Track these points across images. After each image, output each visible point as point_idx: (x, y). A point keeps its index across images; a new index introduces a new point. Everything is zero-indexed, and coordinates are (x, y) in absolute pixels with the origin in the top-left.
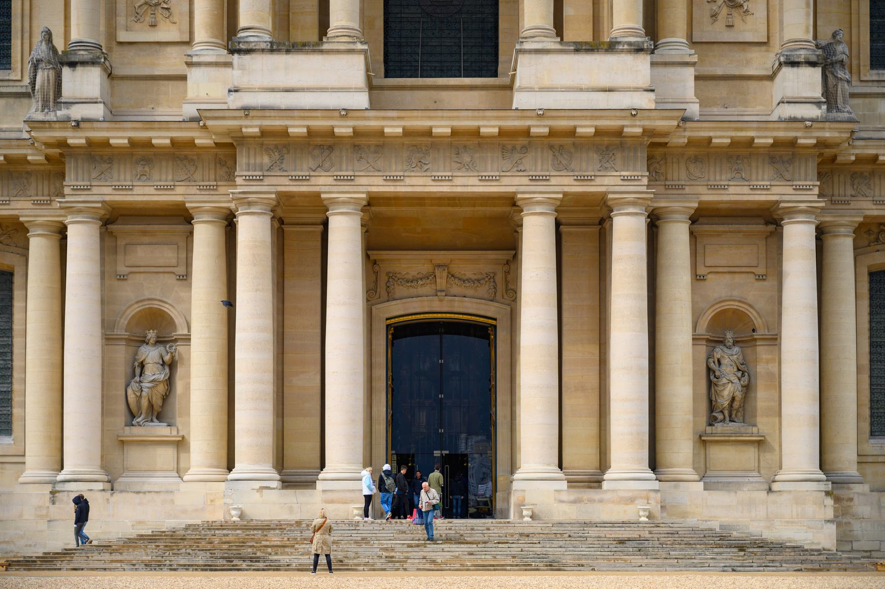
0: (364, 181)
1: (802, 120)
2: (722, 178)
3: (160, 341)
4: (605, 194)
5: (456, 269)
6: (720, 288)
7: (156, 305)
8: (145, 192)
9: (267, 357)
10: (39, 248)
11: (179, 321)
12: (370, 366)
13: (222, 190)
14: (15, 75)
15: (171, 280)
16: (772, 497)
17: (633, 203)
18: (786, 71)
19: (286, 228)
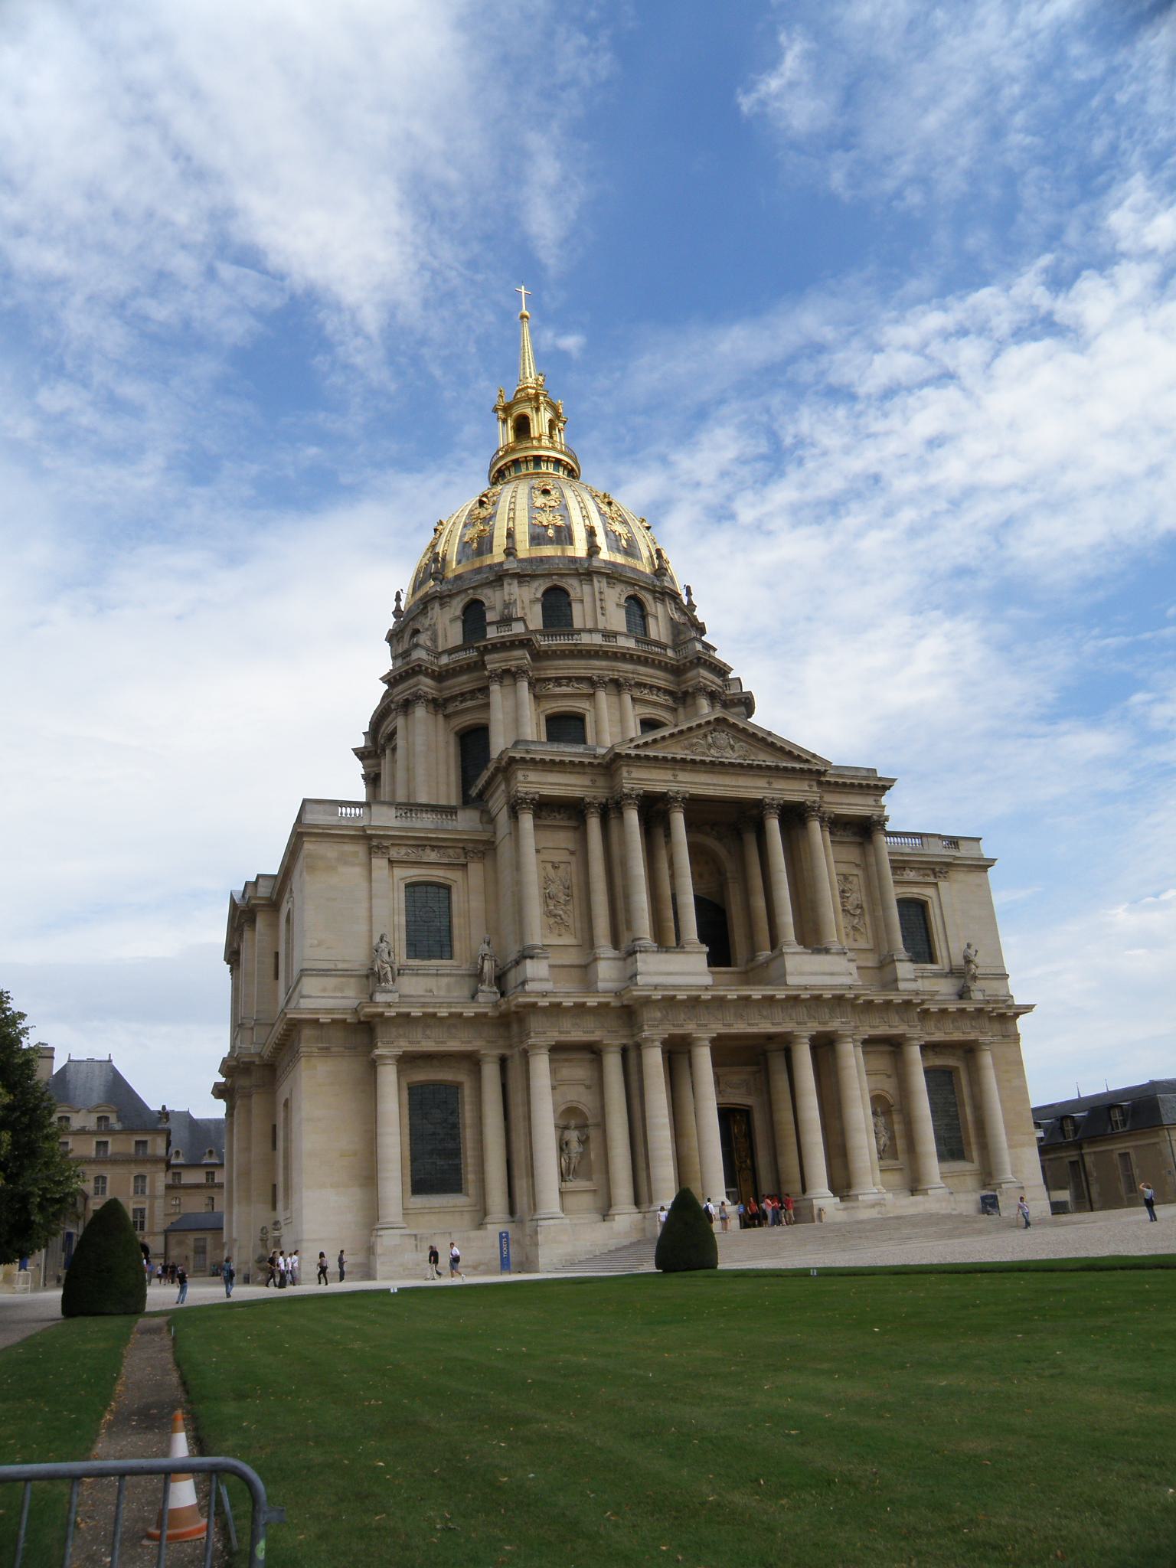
2: (876, 1022)
7: (575, 1105)
8: (577, 1035)
10: (490, 1073)
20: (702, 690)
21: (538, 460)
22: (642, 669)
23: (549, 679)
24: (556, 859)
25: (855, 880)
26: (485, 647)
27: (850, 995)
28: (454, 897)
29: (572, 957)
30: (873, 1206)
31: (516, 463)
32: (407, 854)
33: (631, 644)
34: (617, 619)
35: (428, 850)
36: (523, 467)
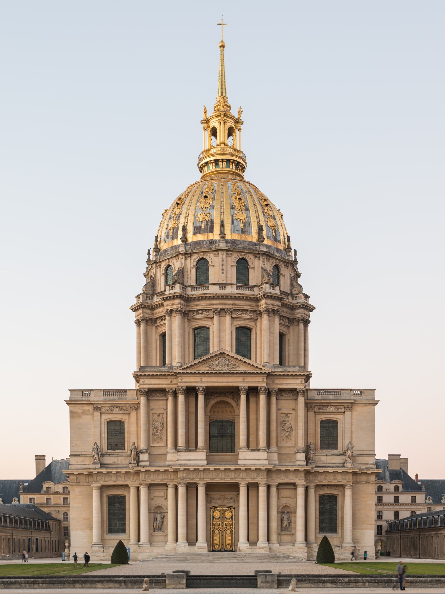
0: (206, 480)
1: (301, 465)
3: (160, 513)
4: (257, 483)
5: (226, 496)
6: (284, 501)
7: (160, 505)
9: (185, 518)
11: (165, 508)
12: (207, 518)
13: (175, 480)
14: (126, 451)
15: (163, 500)
16: (294, 547)
17: (264, 484)
18: (298, 454)
19: (189, 488)
20: (267, 311)
21: (217, 162)
22: (237, 302)
23: (194, 311)
24: (158, 413)
25: (291, 416)
26: (163, 298)
27: (263, 468)
28: (126, 426)
29: (162, 451)
30: (263, 548)
31: (206, 163)
32: (107, 410)
33: (231, 290)
34: (232, 275)
35: (115, 408)
36: (210, 165)
